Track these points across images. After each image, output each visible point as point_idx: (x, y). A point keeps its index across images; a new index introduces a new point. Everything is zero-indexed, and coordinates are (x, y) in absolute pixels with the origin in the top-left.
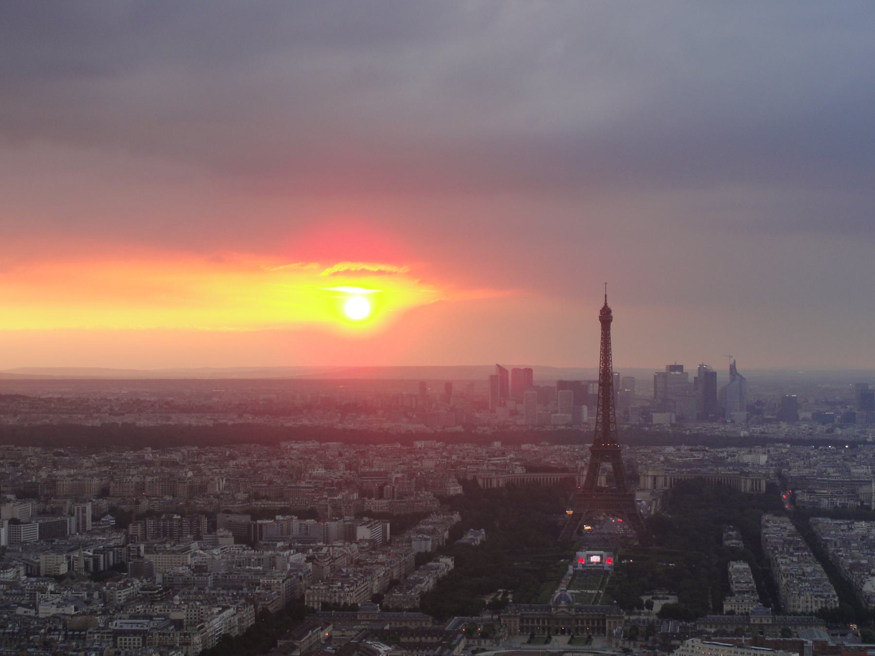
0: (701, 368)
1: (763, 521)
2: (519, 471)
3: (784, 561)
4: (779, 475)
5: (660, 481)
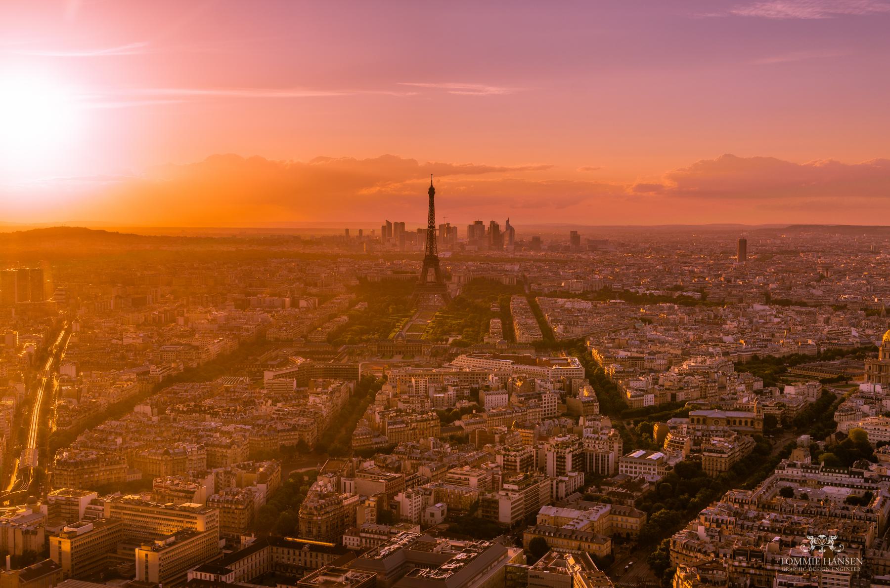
0: (493, 222)
2: (389, 273)
4: (524, 276)
5: (462, 279)
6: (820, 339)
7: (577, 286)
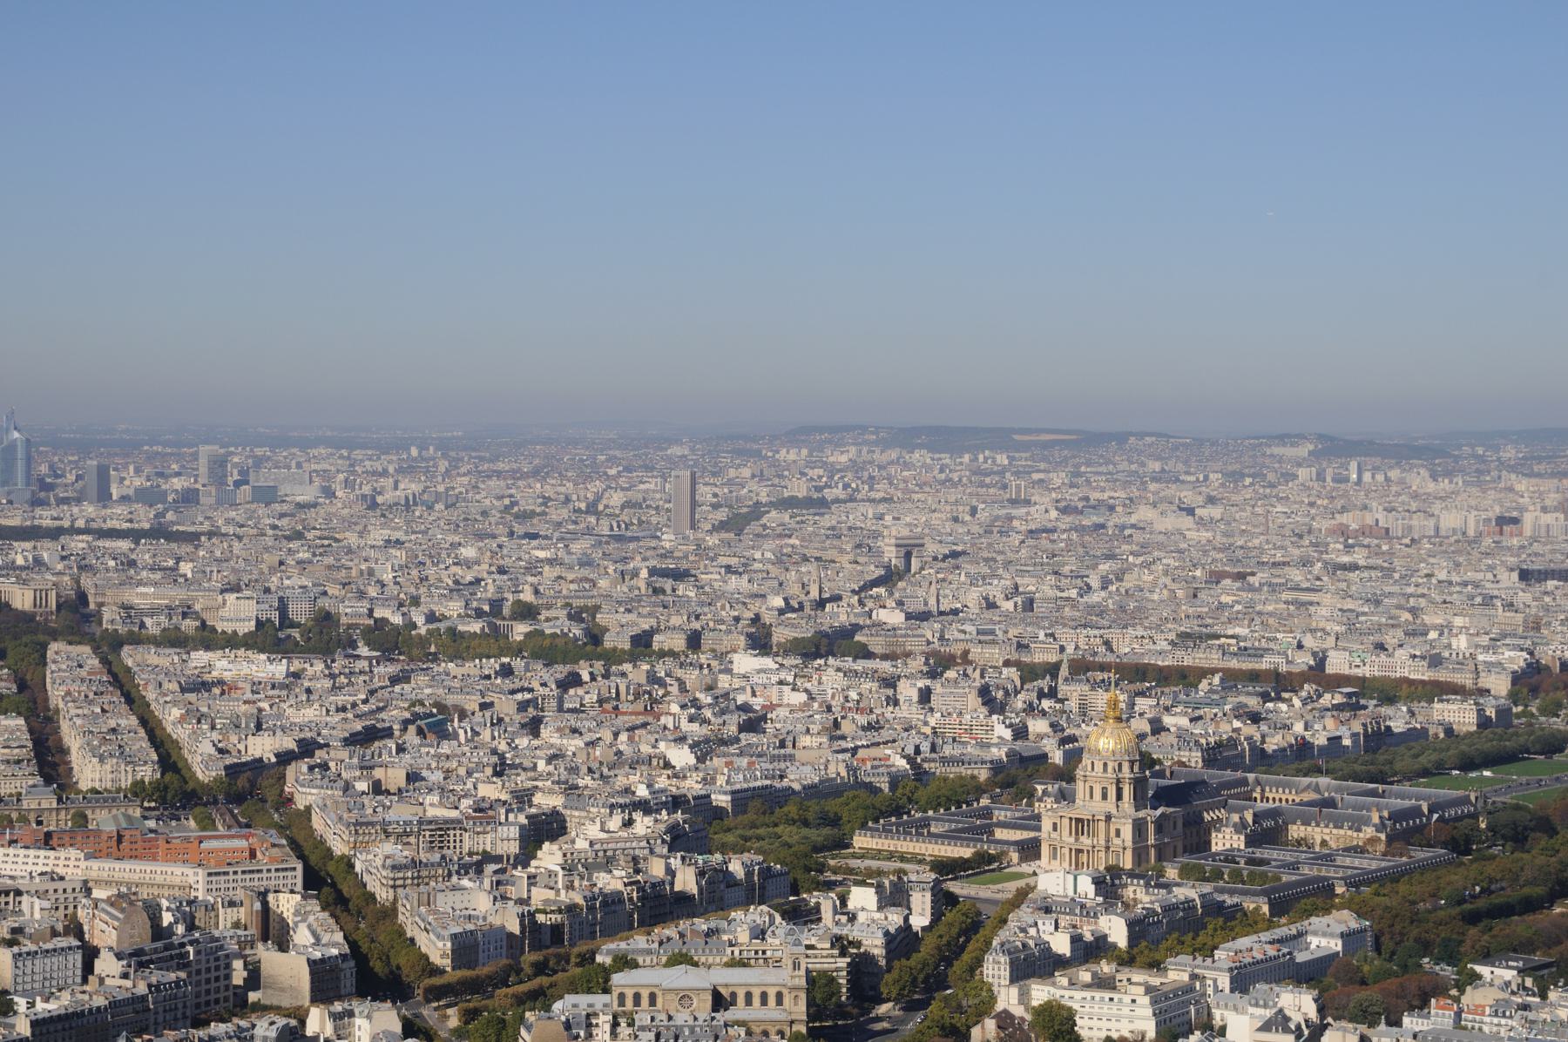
1: (50, 654)
3: (80, 711)
6: (917, 751)
7: (238, 614)
